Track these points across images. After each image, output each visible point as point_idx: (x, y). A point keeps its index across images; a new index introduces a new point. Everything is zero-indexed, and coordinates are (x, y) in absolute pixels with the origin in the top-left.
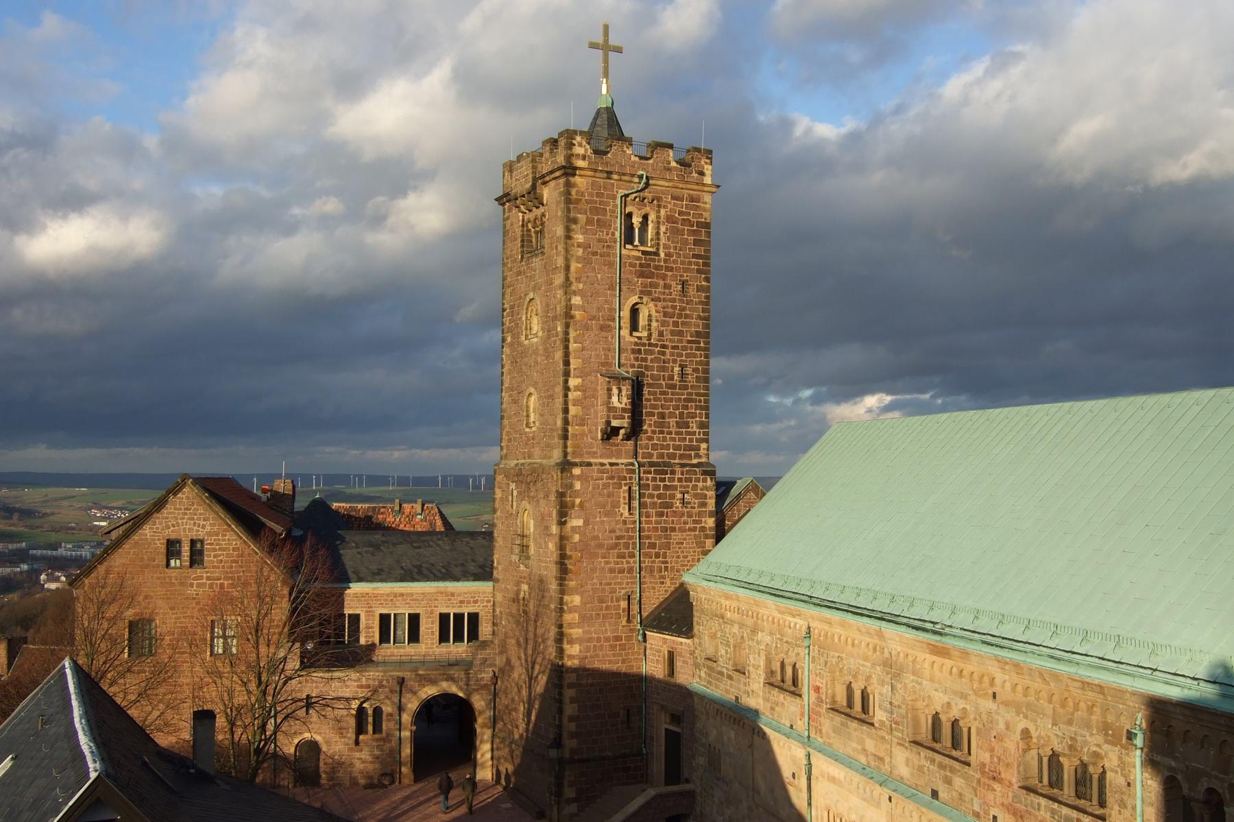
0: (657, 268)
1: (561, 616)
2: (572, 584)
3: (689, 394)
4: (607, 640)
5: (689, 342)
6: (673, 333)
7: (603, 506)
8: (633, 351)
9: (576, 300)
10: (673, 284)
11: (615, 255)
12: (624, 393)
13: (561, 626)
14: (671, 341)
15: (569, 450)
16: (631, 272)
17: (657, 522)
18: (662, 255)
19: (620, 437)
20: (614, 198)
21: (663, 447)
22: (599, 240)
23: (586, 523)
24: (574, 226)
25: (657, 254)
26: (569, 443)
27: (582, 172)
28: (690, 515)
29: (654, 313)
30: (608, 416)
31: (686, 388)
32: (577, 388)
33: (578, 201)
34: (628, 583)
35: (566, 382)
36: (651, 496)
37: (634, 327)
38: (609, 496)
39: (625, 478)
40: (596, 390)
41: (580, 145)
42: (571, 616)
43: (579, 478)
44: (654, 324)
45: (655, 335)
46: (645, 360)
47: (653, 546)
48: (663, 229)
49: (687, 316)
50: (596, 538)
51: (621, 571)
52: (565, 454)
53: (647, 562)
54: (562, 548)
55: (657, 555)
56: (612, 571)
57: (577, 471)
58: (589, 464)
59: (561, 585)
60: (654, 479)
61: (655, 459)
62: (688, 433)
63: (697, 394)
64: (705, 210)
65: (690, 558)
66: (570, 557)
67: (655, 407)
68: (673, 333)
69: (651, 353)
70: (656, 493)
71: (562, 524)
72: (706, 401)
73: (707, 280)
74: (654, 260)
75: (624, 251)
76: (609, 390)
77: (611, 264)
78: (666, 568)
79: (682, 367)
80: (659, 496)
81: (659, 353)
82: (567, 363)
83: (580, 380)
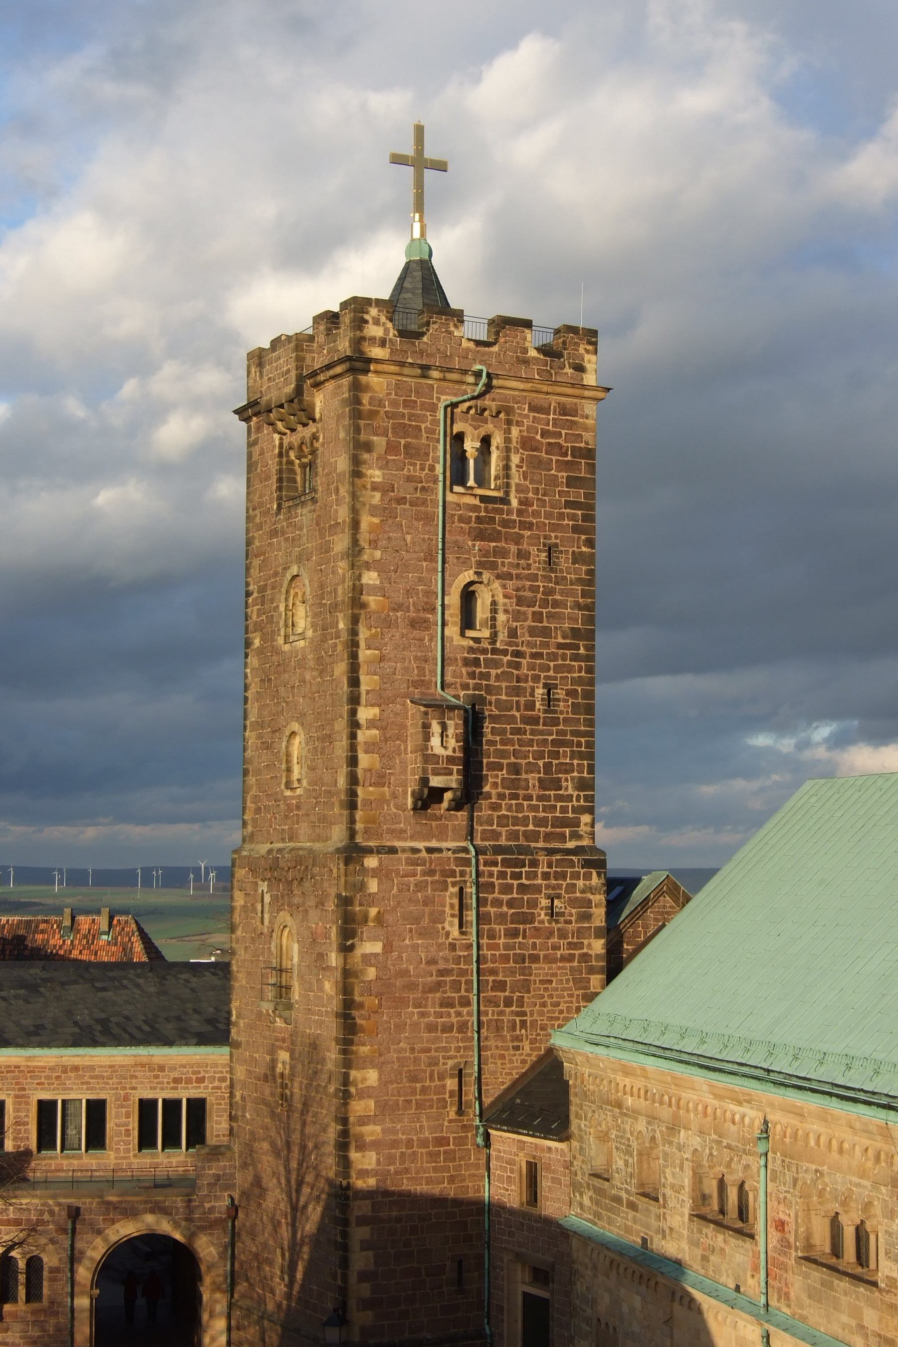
0: (506, 524)
1: (346, 1104)
2: (364, 1050)
3: (559, 733)
4: (424, 1143)
5: (560, 646)
6: (532, 631)
7: (417, 920)
8: (467, 662)
9: (370, 578)
10: (533, 550)
11: (435, 503)
12: (451, 731)
13: (344, 1121)
14: (529, 644)
15: (359, 826)
16: (462, 532)
17: (507, 947)
18: (515, 503)
19: (445, 805)
20: (434, 408)
21: (516, 821)
22: (409, 479)
23: (388, 947)
24: (366, 456)
25: (505, 501)
26: (359, 815)
27: (380, 367)
28: (563, 935)
29: (500, 599)
30: (425, 770)
31: (555, 722)
32: (371, 724)
33: (373, 414)
34: (458, 1049)
35: (353, 713)
36: (498, 903)
37: (468, 621)
38: (425, 904)
39: (453, 874)
40: (403, 727)
41: (377, 322)
42: (362, 1103)
43: (375, 873)
44: (501, 617)
45: (502, 636)
46: (487, 676)
47: (500, 986)
48: (515, 459)
49: (556, 604)
50: (405, 973)
51: (447, 1028)
52: (352, 834)
53: (490, 1014)
54: (346, 990)
55: (508, 1002)
56: (431, 1028)
57: (371, 862)
58: (393, 850)
59: (345, 1052)
60: (502, 875)
61: (503, 842)
62: (559, 798)
63: (576, 733)
64: (586, 428)
65: (563, 1006)
66: (361, 1006)
67: (503, 754)
68: (532, 631)
69: (496, 664)
70: (505, 897)
71: (346, 949)
72: (590, 745)
73: (590, 543)
74: (501, 512)
75: (450, 497)
76: (426, 726)
77: (429, 519)
78: (523, 1024)
79: (549, 688)
80: (511, 904)
81: (510, 664)
82: (354, 682)
83: (376, 710)
